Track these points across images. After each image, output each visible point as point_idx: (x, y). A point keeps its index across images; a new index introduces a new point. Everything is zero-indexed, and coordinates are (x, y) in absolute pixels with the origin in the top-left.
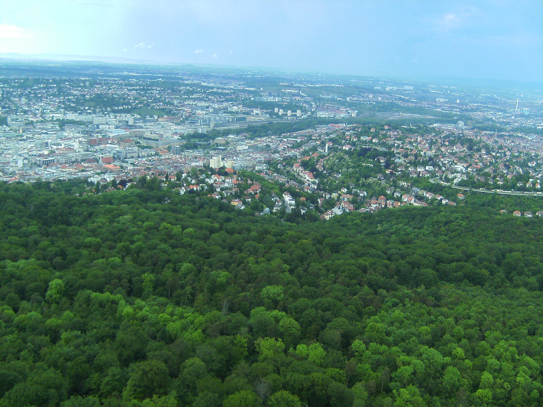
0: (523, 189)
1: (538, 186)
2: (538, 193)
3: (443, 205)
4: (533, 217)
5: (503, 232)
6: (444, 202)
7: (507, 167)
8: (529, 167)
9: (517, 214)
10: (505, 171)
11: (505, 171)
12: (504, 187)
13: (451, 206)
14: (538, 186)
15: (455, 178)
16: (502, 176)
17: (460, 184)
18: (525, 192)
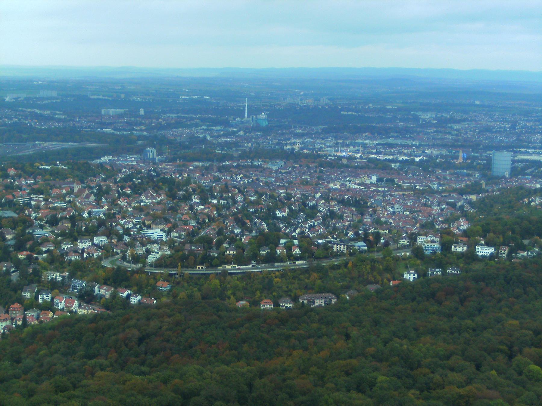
0: (271, 259)
1: (297, 251)
2: (297, 262)
3: (133, 306)
5: (244, 342)
6: (134, 300)
7: (241, 223)
8: (278, 218)
9: (267, 306)
10: (237, 231)
11: (237, 231)
12: (239, 260)
13: (148, 307)
15: (149, 252)
16: (233, 240)
17: (159, 264)
18: (276, 264)
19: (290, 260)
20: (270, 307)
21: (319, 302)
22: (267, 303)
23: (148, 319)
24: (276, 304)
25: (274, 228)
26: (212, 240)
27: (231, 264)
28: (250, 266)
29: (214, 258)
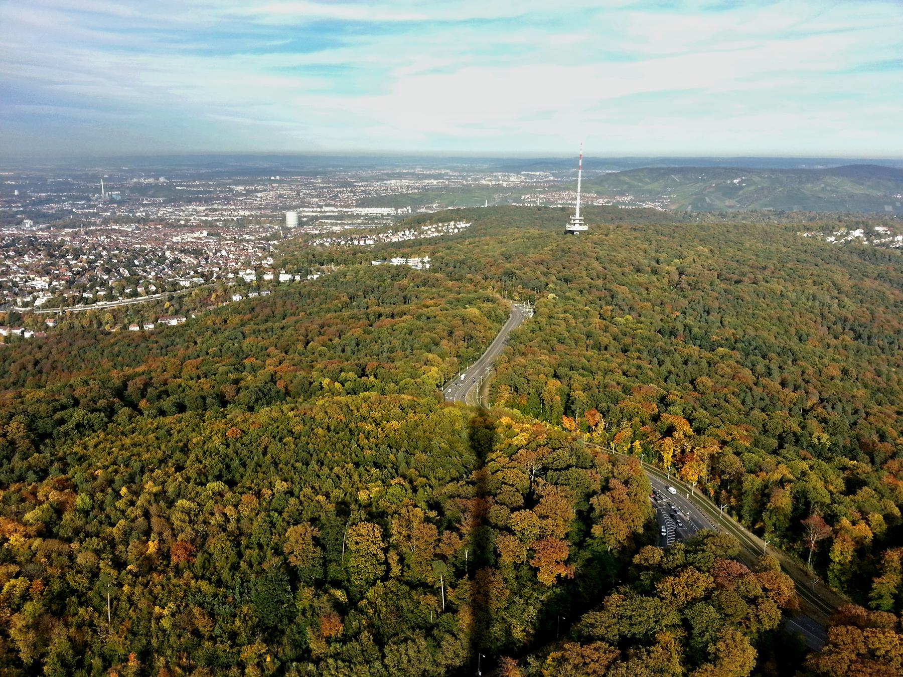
0: (135, 294)
1: (153, 288)
2: (154, 296)
3: (27, 340)
4: (156, 328)
5: (118, 356)
6: (27, 335)
7: (108, 271)
8: (136, 266)
9: (135, 328)
10: (105, 277)
11: (105, 277)
12: (110, 297)
13: (38, 339)
14: (153, 288)
15: (35, 299)
16: (103, 284)
17: (45, 306)
18: (138, 299)
19: (148, 294)
20: (137, 329)
21: (174, 322)
22: (134, 326)
23: (40, 348)
24: (141, 327)
25: (133, 273)
26: (86, 285)
27: (102, 301)
28: (118, 302)
29: (87, 299)
